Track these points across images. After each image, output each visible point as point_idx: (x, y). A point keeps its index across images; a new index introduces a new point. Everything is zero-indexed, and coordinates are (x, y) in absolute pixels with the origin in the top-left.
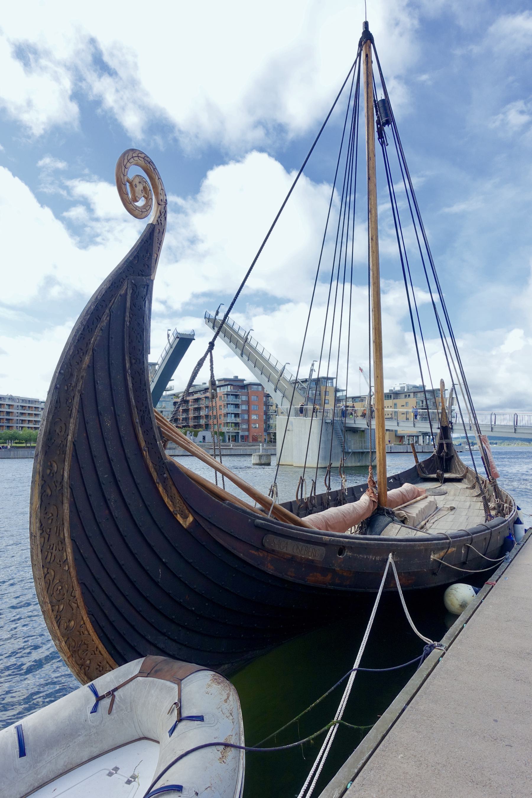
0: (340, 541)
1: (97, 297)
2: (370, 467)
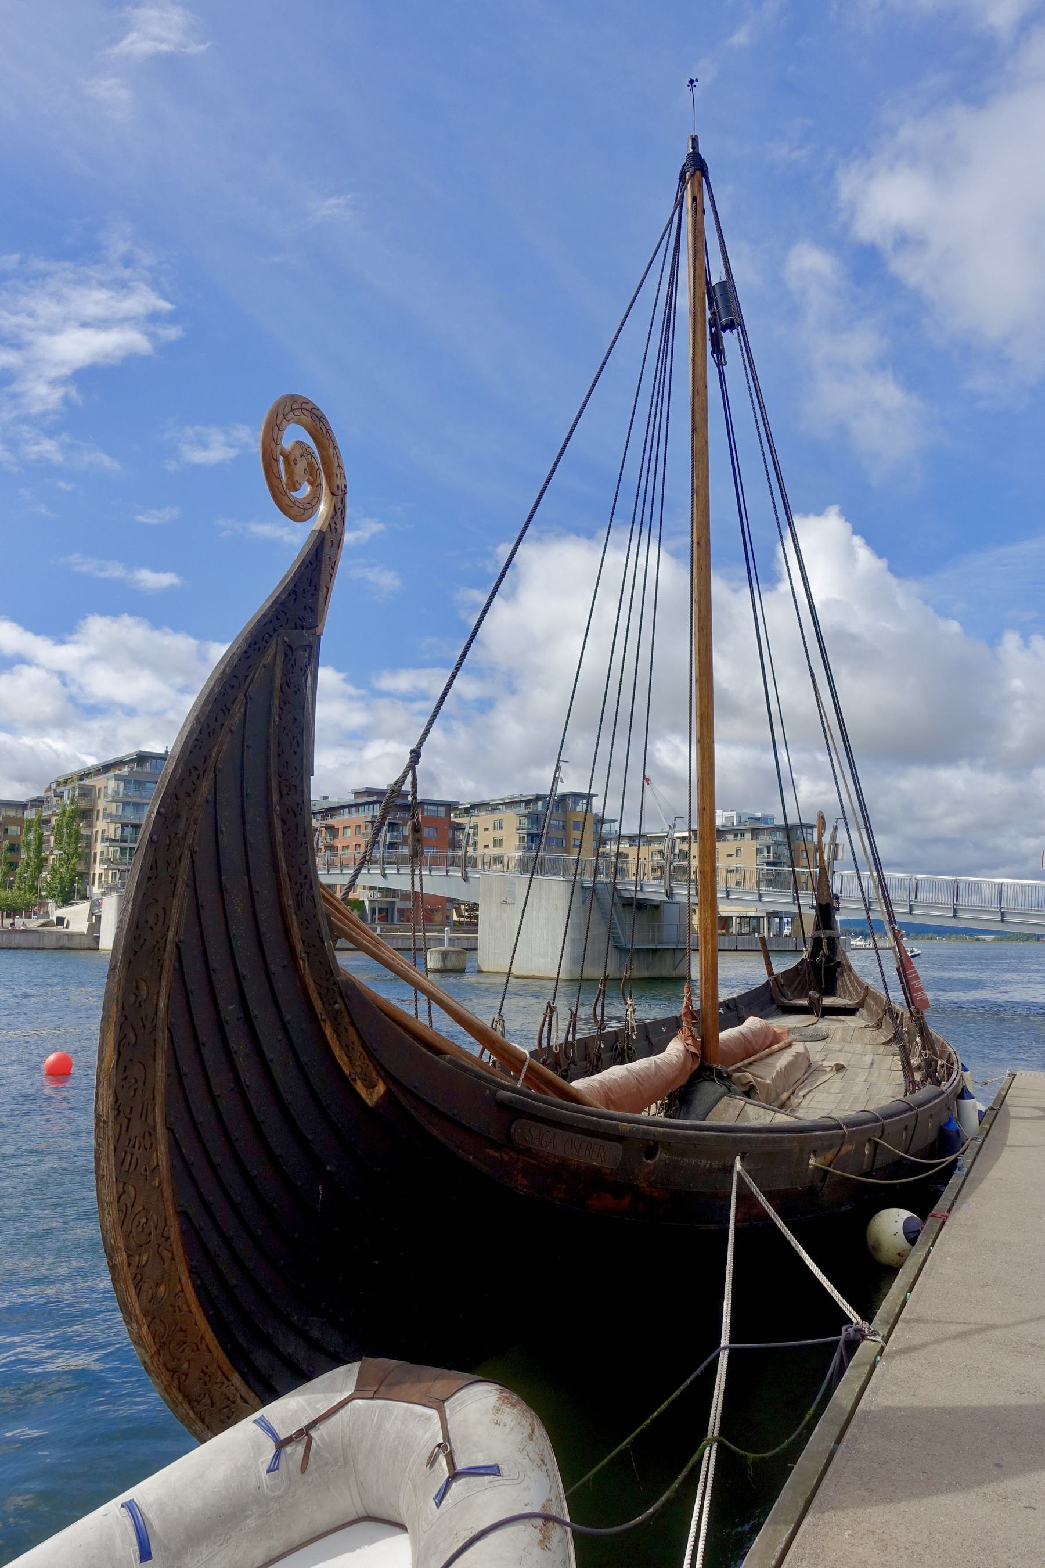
0: (648, 1133)
1: (224, 670)
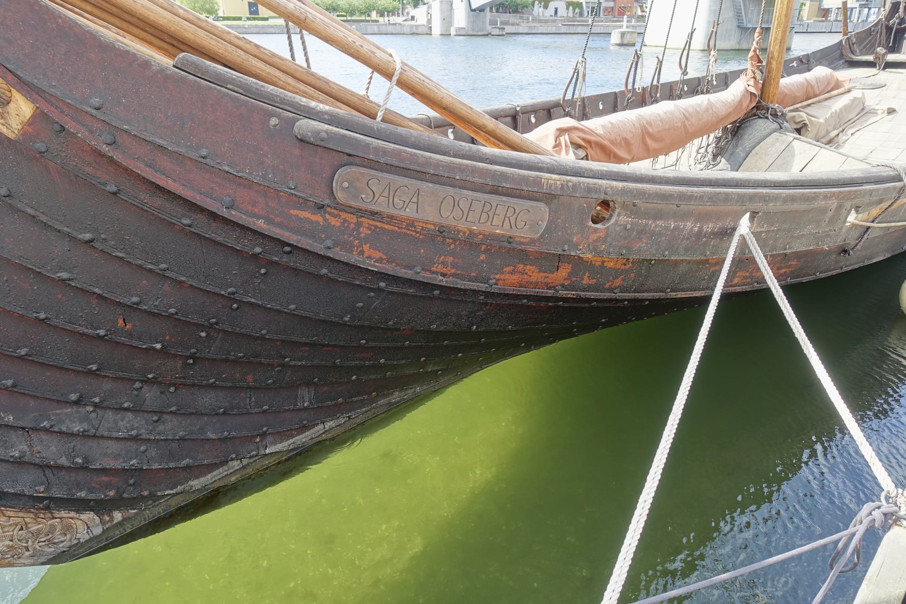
2: (758, 30)
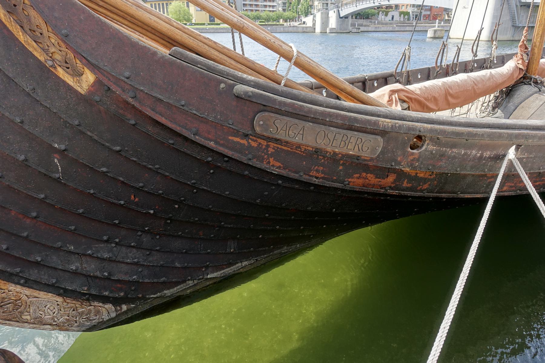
2: (526, 28)
